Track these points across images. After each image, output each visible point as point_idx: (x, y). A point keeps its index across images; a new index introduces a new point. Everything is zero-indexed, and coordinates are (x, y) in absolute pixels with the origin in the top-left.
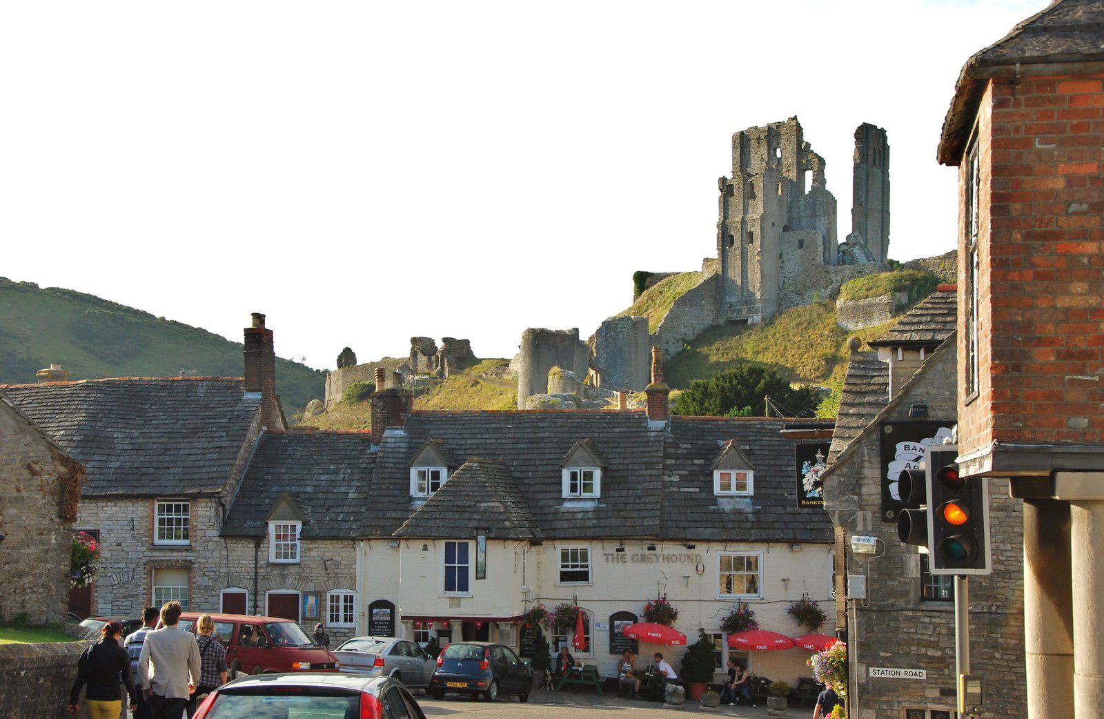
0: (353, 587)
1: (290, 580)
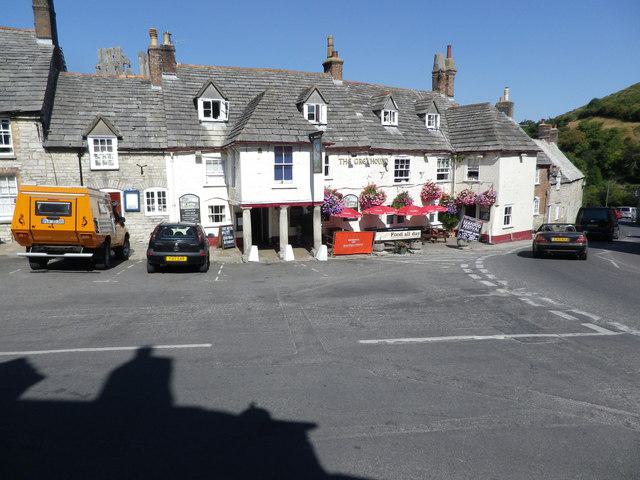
0: (165, 185)
1: (111, 183)
